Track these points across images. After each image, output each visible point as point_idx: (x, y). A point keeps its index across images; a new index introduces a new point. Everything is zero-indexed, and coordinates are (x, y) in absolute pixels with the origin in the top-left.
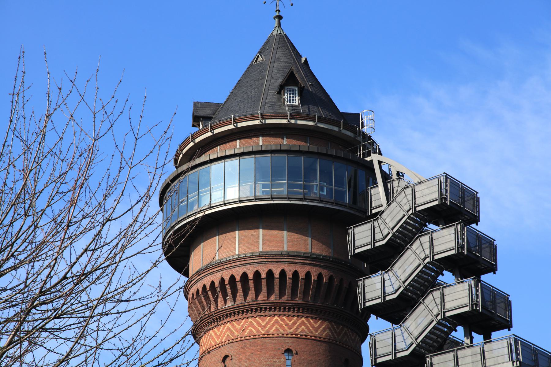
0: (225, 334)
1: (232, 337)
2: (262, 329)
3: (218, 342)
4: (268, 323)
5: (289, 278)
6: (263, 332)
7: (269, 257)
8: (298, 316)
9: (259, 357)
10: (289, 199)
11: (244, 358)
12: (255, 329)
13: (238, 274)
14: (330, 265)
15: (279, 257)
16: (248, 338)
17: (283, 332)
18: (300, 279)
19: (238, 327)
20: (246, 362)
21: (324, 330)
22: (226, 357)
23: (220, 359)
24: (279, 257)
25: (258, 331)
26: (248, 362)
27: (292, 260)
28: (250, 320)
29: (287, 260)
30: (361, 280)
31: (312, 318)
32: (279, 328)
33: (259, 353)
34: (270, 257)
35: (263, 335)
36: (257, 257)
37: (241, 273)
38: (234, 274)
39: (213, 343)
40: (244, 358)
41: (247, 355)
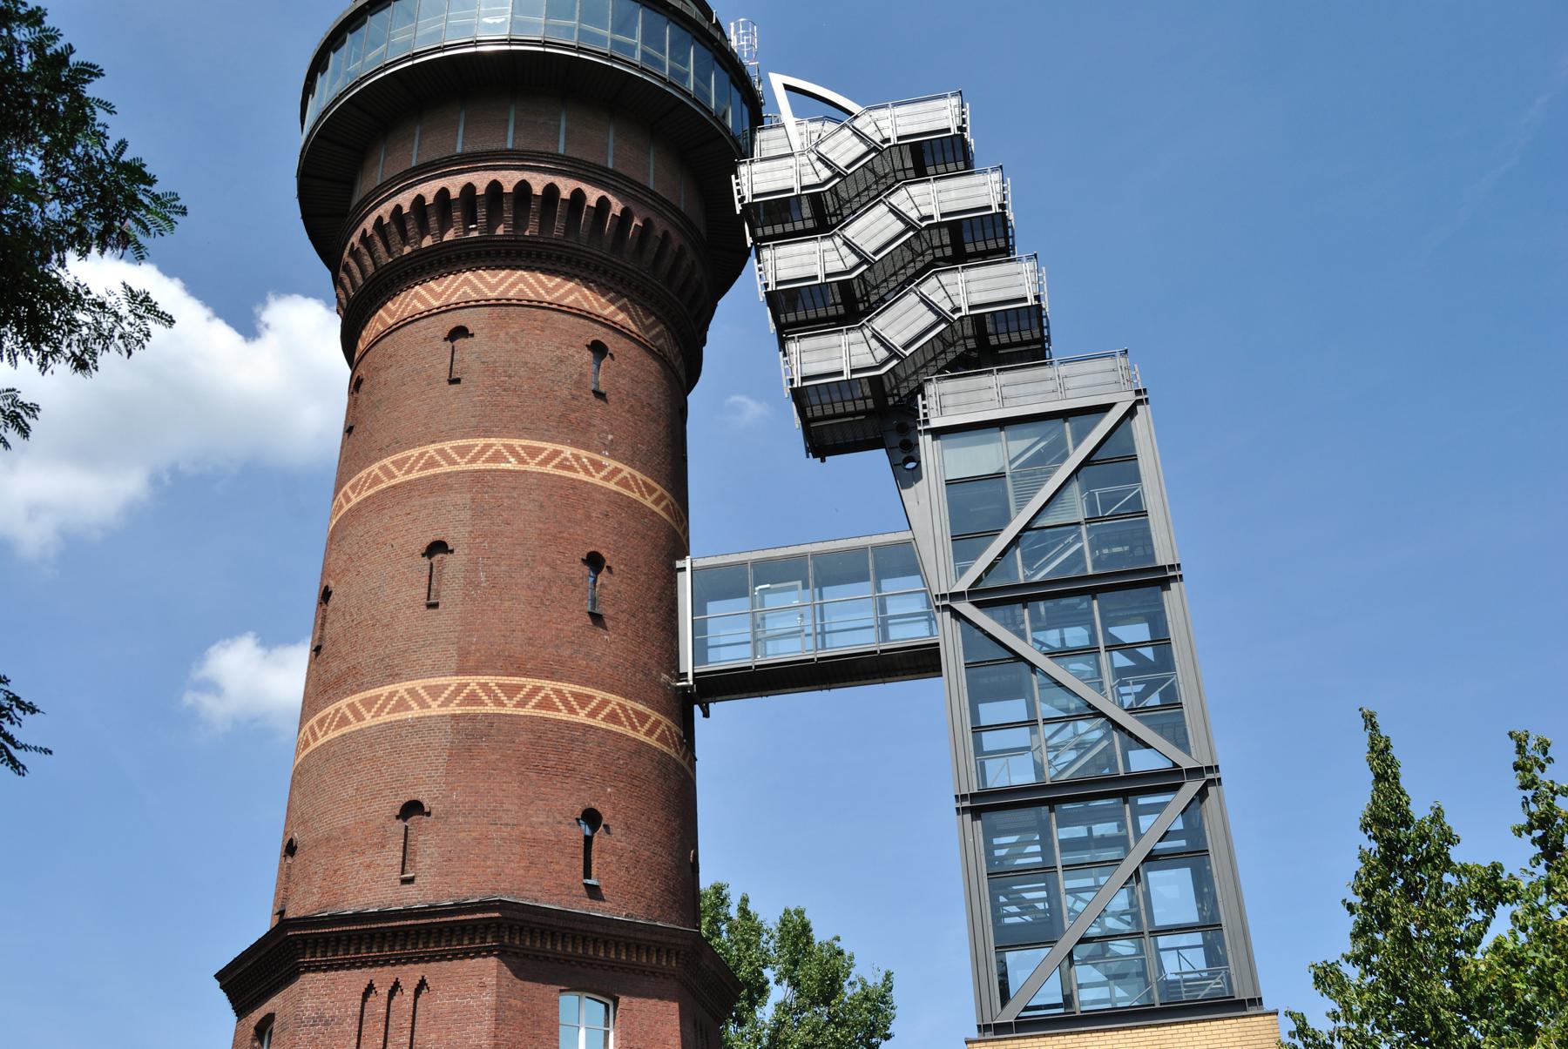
0: (457, 289)
1: (475, 296)
2: (546, 292)
3: (436, 304)
4: (557, 287)
5: (613, 215)
6: (548, 299)
7: (579, 166)
8: (617, 292)
9: (538, 340)
10: (642, 70)
11: (502, 335)
12: (531, 290)
13: (509, 181)
14: (682, 226)
15: (599, 172)
16: (514, 302)
17: (590, 310)
18: (633, 225)
19: (493, 281)
20: (507, 343)
21: (657, 336)
22: (459, 332)
23: (439, 333)
24: (599, 172)
25: (537, 293)
26: (512, 345)
27: (623, 187)
28: (520, 273)
29: (615, 183)
30: (768, 246)
31: (640, 305)
32: (580, 298)
33: (538, 332)
34: (583, 167)
35: (549, 303)
36: (557, 159)
37: (516, 181)
38: (499, 179)
39: (422, 308)
40: (502, 335)
41: (511, 332)
